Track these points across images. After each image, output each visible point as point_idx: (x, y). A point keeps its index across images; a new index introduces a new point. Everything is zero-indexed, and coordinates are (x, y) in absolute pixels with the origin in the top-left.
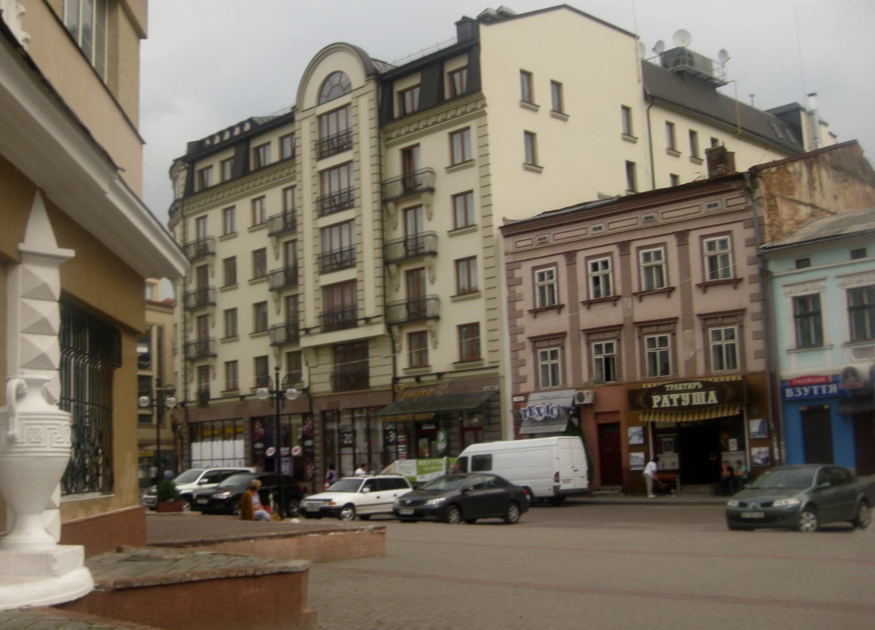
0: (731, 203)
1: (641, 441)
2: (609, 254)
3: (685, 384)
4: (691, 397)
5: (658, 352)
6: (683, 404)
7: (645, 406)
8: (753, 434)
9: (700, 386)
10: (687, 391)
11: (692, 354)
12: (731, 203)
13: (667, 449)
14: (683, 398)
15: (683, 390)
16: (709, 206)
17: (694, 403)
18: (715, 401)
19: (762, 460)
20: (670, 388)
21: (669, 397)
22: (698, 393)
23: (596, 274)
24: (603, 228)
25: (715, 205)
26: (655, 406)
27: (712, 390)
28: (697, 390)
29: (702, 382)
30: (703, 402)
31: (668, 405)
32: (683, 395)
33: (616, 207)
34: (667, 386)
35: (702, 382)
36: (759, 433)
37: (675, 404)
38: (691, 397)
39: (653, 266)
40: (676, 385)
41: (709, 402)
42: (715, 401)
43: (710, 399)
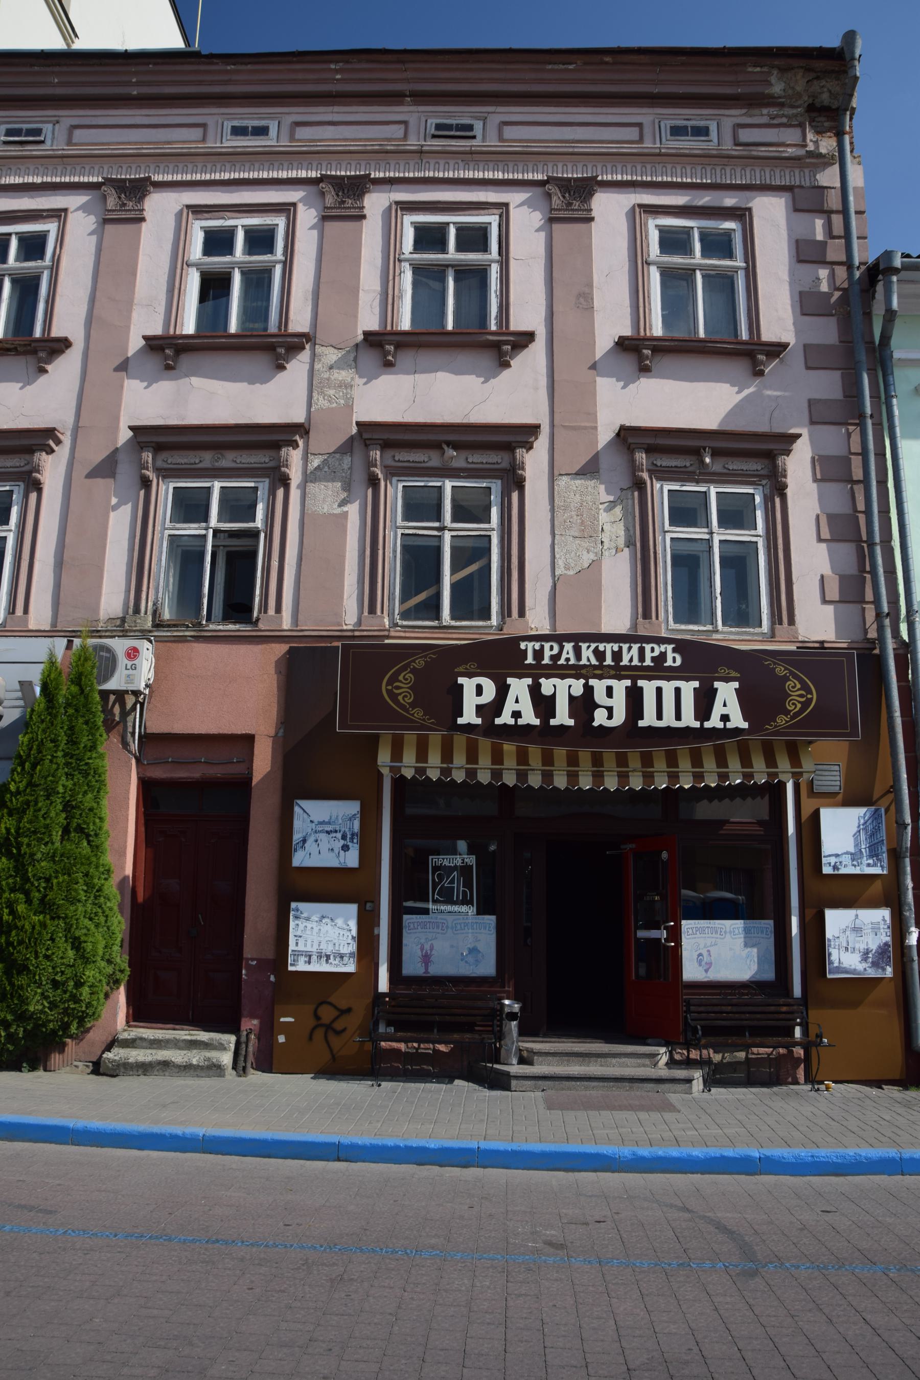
0: (745, 135)
1: (352, 859)
2: (287, 209)
3: (609, 648)
4: (635, 698)
5: (447, 536)
6: (600, 718)
7: (418, 714)
8: (833, 860)
9: (673, 660)
10: (618, 672)
11: (587, 558)
12: (745, 135)
13: (448, 897)
14: (600, 696)
15: (601, 667)
16: (677, 131)
17: (649, 719)
18: (738, 721)
19: (865, 955)
20: (538, 654)
21: (535, 690)
22: (668, 687)
23: (218, 261)
24: (273, 132)
25: (702, 132)
26: (469, 716)
27: (727, 680)
28: (659, 670)
29: (681, 646)
30: (689, 719)
31: (530, 718)
32: (599, 686)
33: (337, 71)
34: (530, 647)
35: (681, 646)
36: (855, 857)
37: (562, 717)
38: (635, 698)
39: (447, 266)
40: (568, 647)
41: (714, 722)
42: (738, 721)
43: (718, 710)
